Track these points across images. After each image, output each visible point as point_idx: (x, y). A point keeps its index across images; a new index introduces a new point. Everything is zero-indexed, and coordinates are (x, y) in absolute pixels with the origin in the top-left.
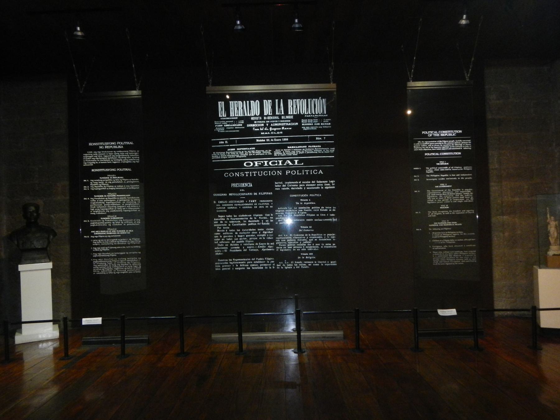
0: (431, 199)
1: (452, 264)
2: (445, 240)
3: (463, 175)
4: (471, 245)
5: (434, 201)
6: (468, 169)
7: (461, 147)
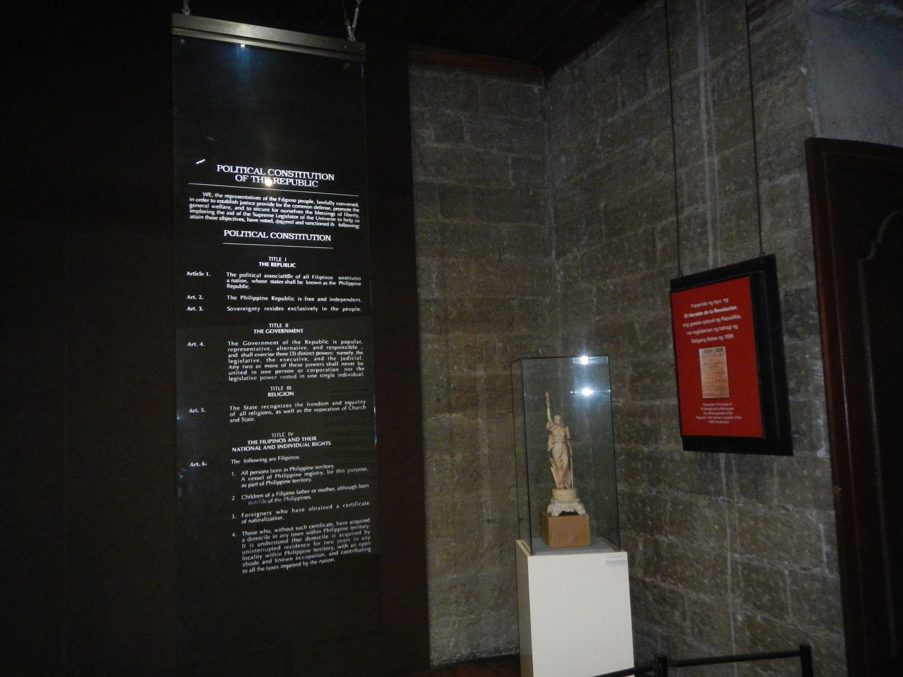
0: (241, 369)
1: (299, 564)
2: (281, 494)
3: (337, 300)
4: (356, 504)
5: (249, 374)
6: (352, 284)
7: (330, 222)
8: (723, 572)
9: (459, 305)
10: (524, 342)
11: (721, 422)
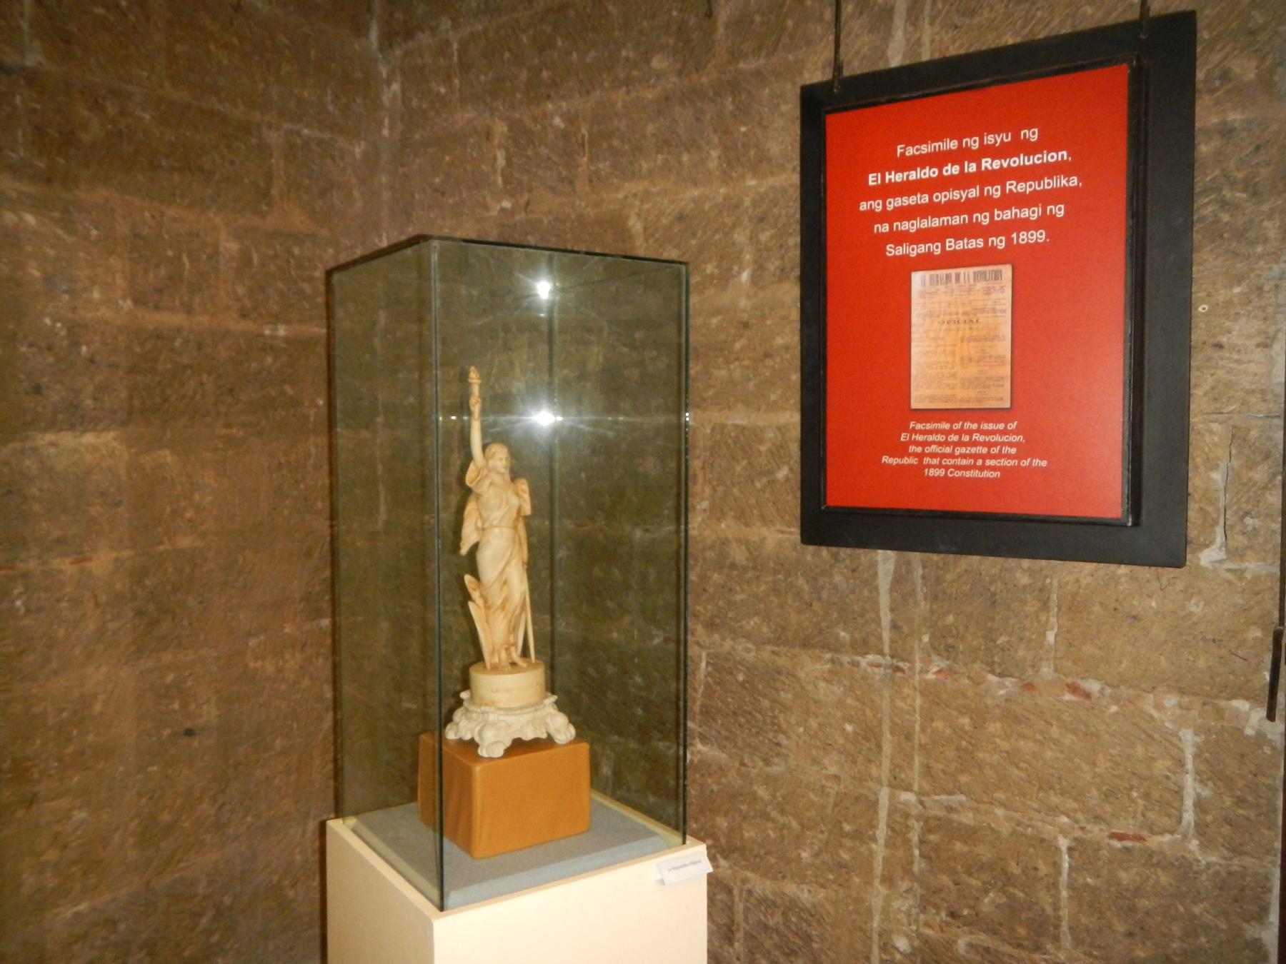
8: (863, 835)
9: (111, 109)
10: (296, 251)
11: (969, 474)
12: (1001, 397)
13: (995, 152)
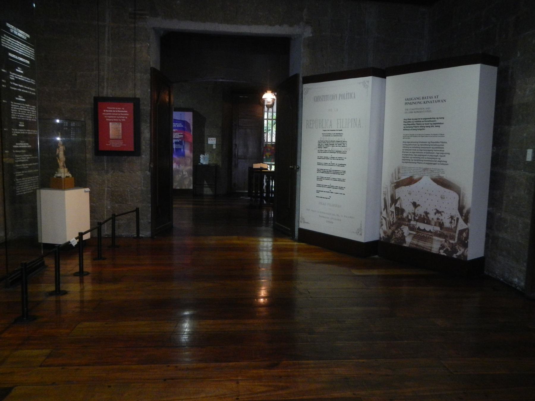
12: (121, 137)
13: (119, 110)
